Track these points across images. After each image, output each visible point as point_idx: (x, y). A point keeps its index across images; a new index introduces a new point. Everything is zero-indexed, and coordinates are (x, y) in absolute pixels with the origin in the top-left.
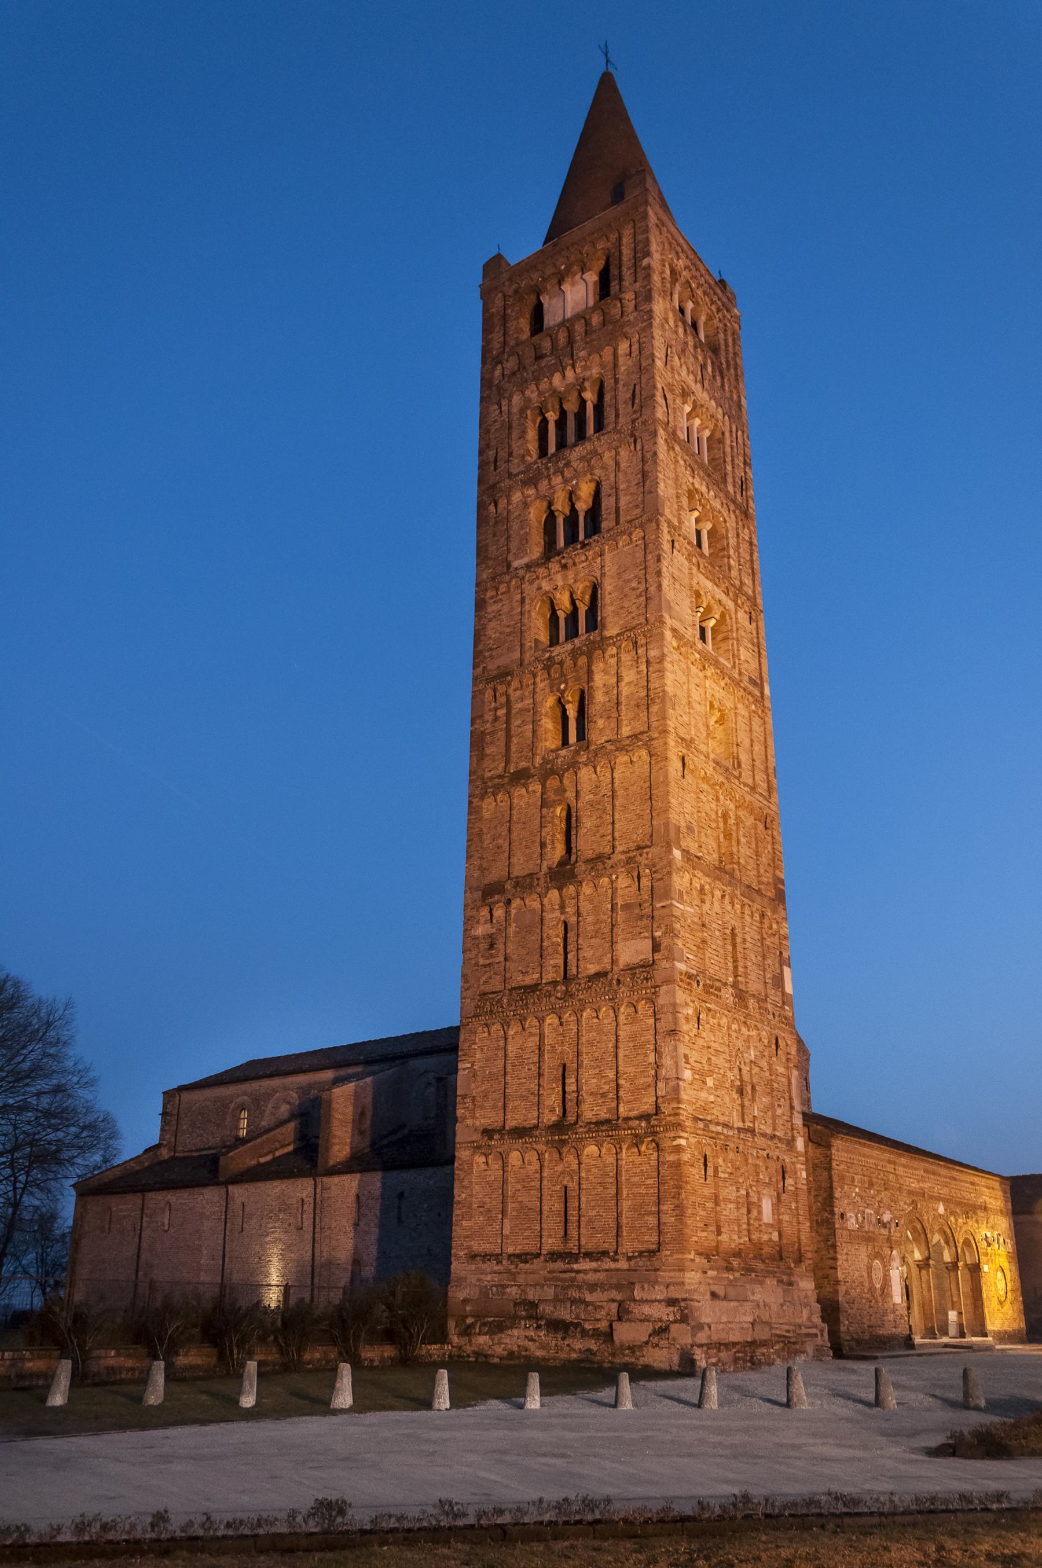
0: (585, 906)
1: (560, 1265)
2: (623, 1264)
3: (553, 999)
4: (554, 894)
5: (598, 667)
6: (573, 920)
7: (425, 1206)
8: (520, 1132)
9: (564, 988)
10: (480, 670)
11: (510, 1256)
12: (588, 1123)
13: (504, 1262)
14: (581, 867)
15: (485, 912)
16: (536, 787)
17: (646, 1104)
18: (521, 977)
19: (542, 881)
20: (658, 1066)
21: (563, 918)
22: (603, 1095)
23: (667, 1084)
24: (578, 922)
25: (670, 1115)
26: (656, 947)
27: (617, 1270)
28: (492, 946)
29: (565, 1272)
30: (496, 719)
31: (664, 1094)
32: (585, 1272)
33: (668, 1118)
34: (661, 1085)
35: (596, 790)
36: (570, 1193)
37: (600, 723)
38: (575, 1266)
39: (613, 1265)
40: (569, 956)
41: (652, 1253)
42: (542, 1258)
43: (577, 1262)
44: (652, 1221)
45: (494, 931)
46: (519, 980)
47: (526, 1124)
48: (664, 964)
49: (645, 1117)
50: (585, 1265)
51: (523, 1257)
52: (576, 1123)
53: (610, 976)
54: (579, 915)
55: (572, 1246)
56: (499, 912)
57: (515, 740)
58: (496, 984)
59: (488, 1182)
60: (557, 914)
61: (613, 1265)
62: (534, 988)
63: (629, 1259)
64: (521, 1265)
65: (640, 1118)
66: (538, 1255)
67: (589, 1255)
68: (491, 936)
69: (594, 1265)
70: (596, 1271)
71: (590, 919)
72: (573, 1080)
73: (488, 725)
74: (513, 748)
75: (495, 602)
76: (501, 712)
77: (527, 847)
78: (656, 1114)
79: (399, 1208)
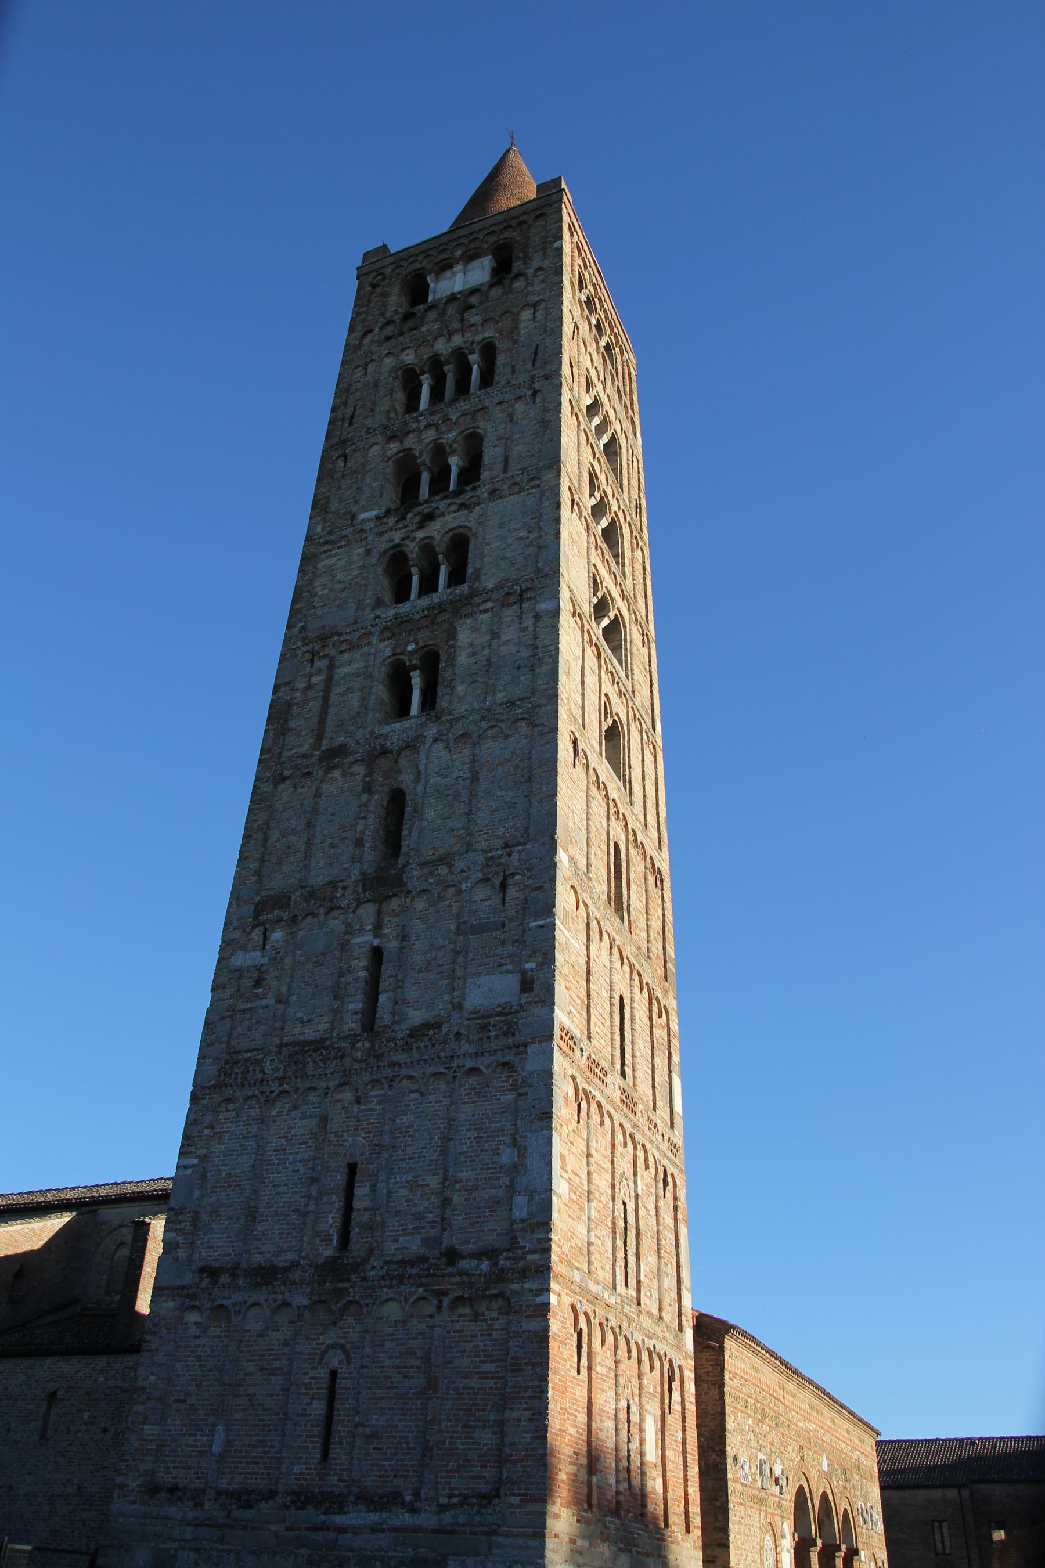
0: (417, 925)
1: (312, 1515)
2: (427, 1519)
3: (347, 1061)
4: (368, 911)
6: (391, 946)
7: (86, 1415)
8: (266, 1276)
9: (367, 1045)
10: (296, 631)
11: (219, 1493)
12: (386, 1263)
13: (207, 1505)
14: (414, 876)
16: (360, 770)
18: (298, 1030)
19: (350, 891)
21: (376, 942)
22: (418, 1216)
23: (531, 1198)
24: (402, 948)
25: (531, 1252)
26: (526, 985)
27: (416, 1530)
28: (258, 982)
29: (315, 1528)
31: (524, 1215)
32: (356, 1531)
33: (529, 1257)
34: (520, 1200)
36: (341, 1383)
37: (461, 689)
38: (338, 1519)
39: (406, 1519)
40: (382, 999)
41: (486, 1499)
42: (279, 1500)
43: (341, 1511)
45: (265, 960)
46: (298, 1032)
47: (280, 1261)
48: (539, 1010)
49: (490, 1254)
50: (357, 1517)
51: (244, 1498)
52: (365, 1261)
53: (445, 1030)
54: (404, 938)
56: (277, 936)
57: (332, 711)
59: (199, 1358)
60: (368, 937)
61: (406, 1519)
62: (318, 1045)
63: (443, 1508)
64: (237, 1513)
66: (272, 1494)
68: (259, 968)
69: (374, 1517)
70: (375, 1529)
71: (418, 945)
72: (367, 1190)
73: (298, 694)
74: (330, 721)
75: (328, 557)
77: (332, 846)
78: (510, 1250)
79: (46, 1416)
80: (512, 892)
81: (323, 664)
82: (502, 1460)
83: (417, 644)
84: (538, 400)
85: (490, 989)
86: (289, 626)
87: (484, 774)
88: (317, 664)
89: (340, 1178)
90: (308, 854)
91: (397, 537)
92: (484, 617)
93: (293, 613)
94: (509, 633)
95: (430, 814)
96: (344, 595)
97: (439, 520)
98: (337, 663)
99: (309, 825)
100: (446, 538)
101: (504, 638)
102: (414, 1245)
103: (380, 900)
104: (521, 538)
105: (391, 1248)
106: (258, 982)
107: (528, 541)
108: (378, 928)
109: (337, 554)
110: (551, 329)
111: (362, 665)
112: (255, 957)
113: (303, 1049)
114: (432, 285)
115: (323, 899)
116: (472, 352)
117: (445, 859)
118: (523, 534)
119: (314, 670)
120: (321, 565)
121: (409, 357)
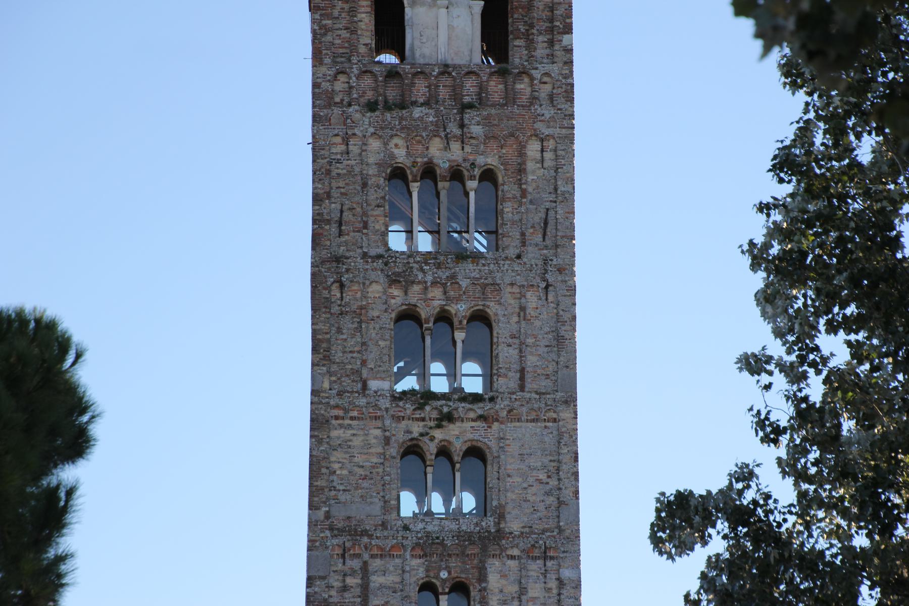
5: (494, 567)
10: (321, 514)
30: (345, 588)
73: (333, 593)
75: (341, 426)
81: (356, 564)
83: (449, 573)
84: (551, 298)
86: (312, 506)
88: (349, 563)
91: (417, 429)
92: (511, 563)
93: (314, 491)
96: (365, 484)
97: (458, 424)
98: (370, 568)
100: (464, 448)
101: (531, 593)
104: (540, 482)
107: (548, 487)
109: (349, 427)
110: (563, 193)
111: (398, 579)
114: (408, 10)
116: (472, 178)
118: (543, 476)
119: (346, 568)
120: (334, 433)
121: (401, 155)
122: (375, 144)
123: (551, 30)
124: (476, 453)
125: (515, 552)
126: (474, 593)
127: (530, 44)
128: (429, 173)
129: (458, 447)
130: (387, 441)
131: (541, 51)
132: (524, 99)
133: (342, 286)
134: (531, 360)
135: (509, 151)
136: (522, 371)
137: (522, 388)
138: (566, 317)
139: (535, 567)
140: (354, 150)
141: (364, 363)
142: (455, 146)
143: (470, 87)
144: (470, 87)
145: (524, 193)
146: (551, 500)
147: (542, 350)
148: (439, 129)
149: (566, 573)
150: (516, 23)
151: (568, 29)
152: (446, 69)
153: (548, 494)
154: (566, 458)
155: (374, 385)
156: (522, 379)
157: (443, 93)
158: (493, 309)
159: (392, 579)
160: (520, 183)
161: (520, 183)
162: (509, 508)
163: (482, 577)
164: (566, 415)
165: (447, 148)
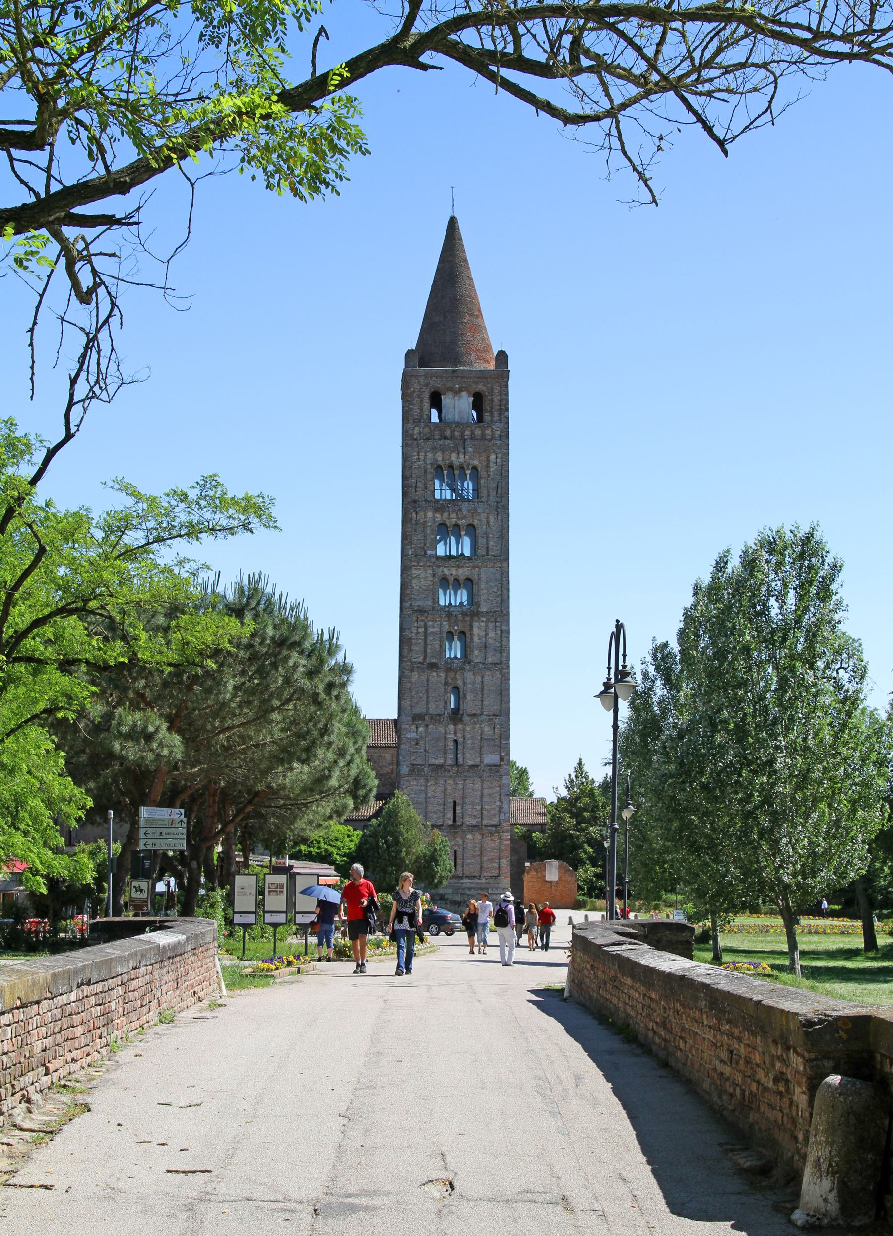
0: (468, 736)
2: (483, 881)
4: (452, 727)
5: (476, 625)
6: (461, 740)
15: (413, 727)
16: (443, 675)
17: (495, 821)
20: (501, 807)
26: (502, 759)
28: (417, 744)
30: (418, 633)
34: (502, 815)
35: (474, 683)
37: (476, 652)
44: (496, 865)
48: (505, 767)
55: (460, 873)
56: (421, 729)
57: (429, 647)
58: (419, 761)
62: (441, 766)
65: (493, 826)
67: (467, 877)
71: (469, 741)
76: (421, 630)
80: (496, 730)
82: (500, 870)
85: (491, 758)
87: (486, 688)
89: (452, 804)
90: (427, 703)
94: (492, 634)
95: (469, 698)
99: (427, 692)
102: (474, 822)
103: (455, 725)
105: (468, 823)
106: (417, 744)
108: (455, 733)
112: (413, 735)
113: (438, 768)
115: (436, 719)
117: (474, 715)
118: (495, 590)
122: (430, 455)
123: (500, 409)
124: (469, 580)
125: (484, 619)
126: (468, 635)
127: (492, 416)
128: (451, 467)
129: (462, 578)
130: (434, 575)
131: (496, 418)
132: (489, 437)
133: (417, 513)
134: (491, 543)
135: (483, 459)
136: (488, 548)
137: (487, 554)
138: (505, 526)
139: (491, 625)
140: (422, 458)
141: (425, 544)
142: (462, 456)
143: (468, 432)
144: (468, 432)
145: (489, 476)
146: (499, 599)
147: (496, 539)
148: (456, 449)
149: (504, 628)
150: (486, 406)
151: (507, 409)
152: (458, 424)
153: (497, 596)
154: (505, 583)
155: (429, 553)
156: (488, 551)
157: (457, 434)
158: (476, 522)
159: (436, 630)
160: (487, 471)
161: (487, 471)
162: (482, 602)
163: (471, 629)
164: (505, 565)
165: (458, 457)
